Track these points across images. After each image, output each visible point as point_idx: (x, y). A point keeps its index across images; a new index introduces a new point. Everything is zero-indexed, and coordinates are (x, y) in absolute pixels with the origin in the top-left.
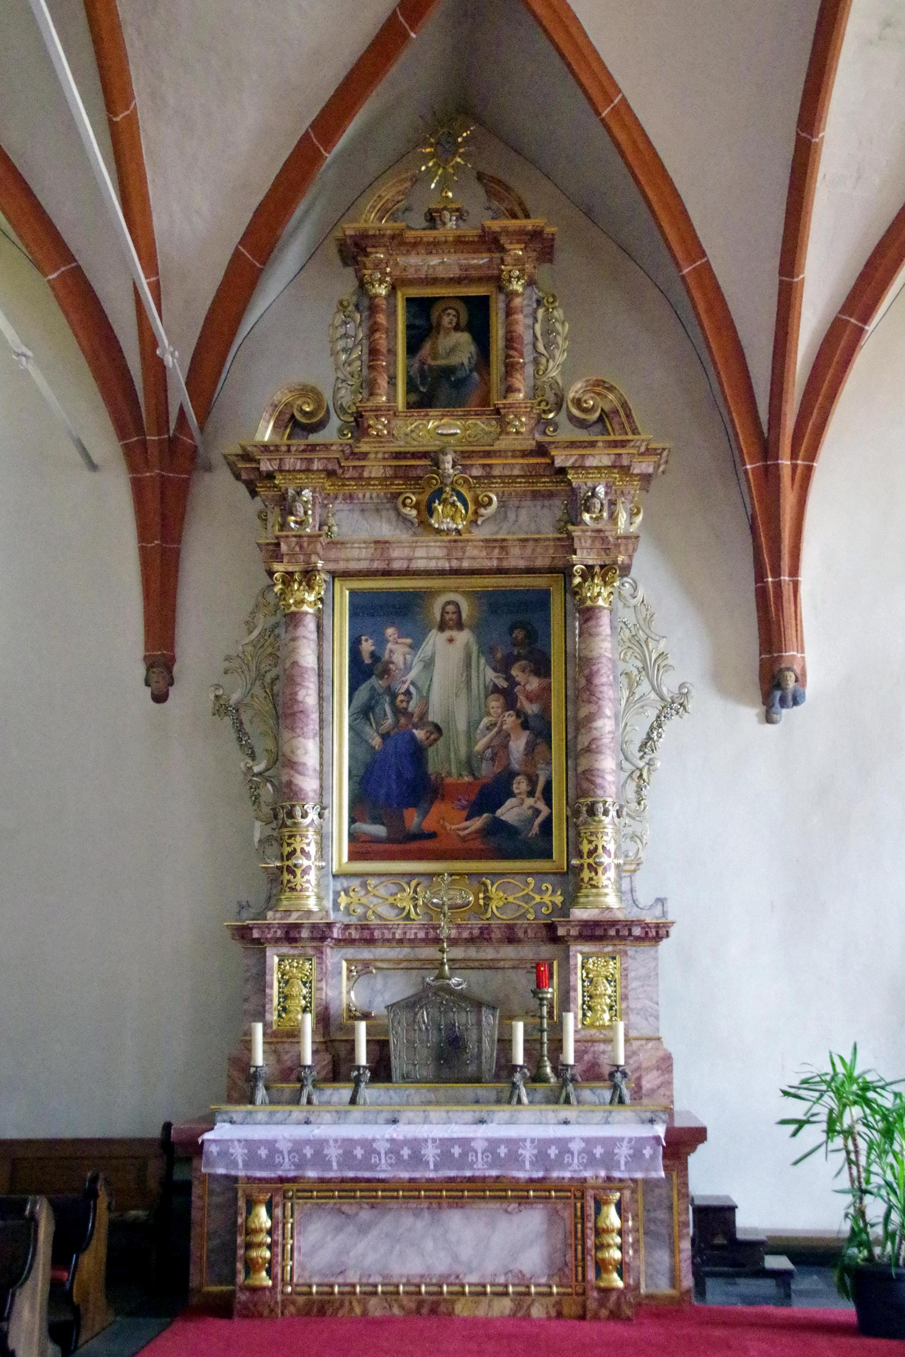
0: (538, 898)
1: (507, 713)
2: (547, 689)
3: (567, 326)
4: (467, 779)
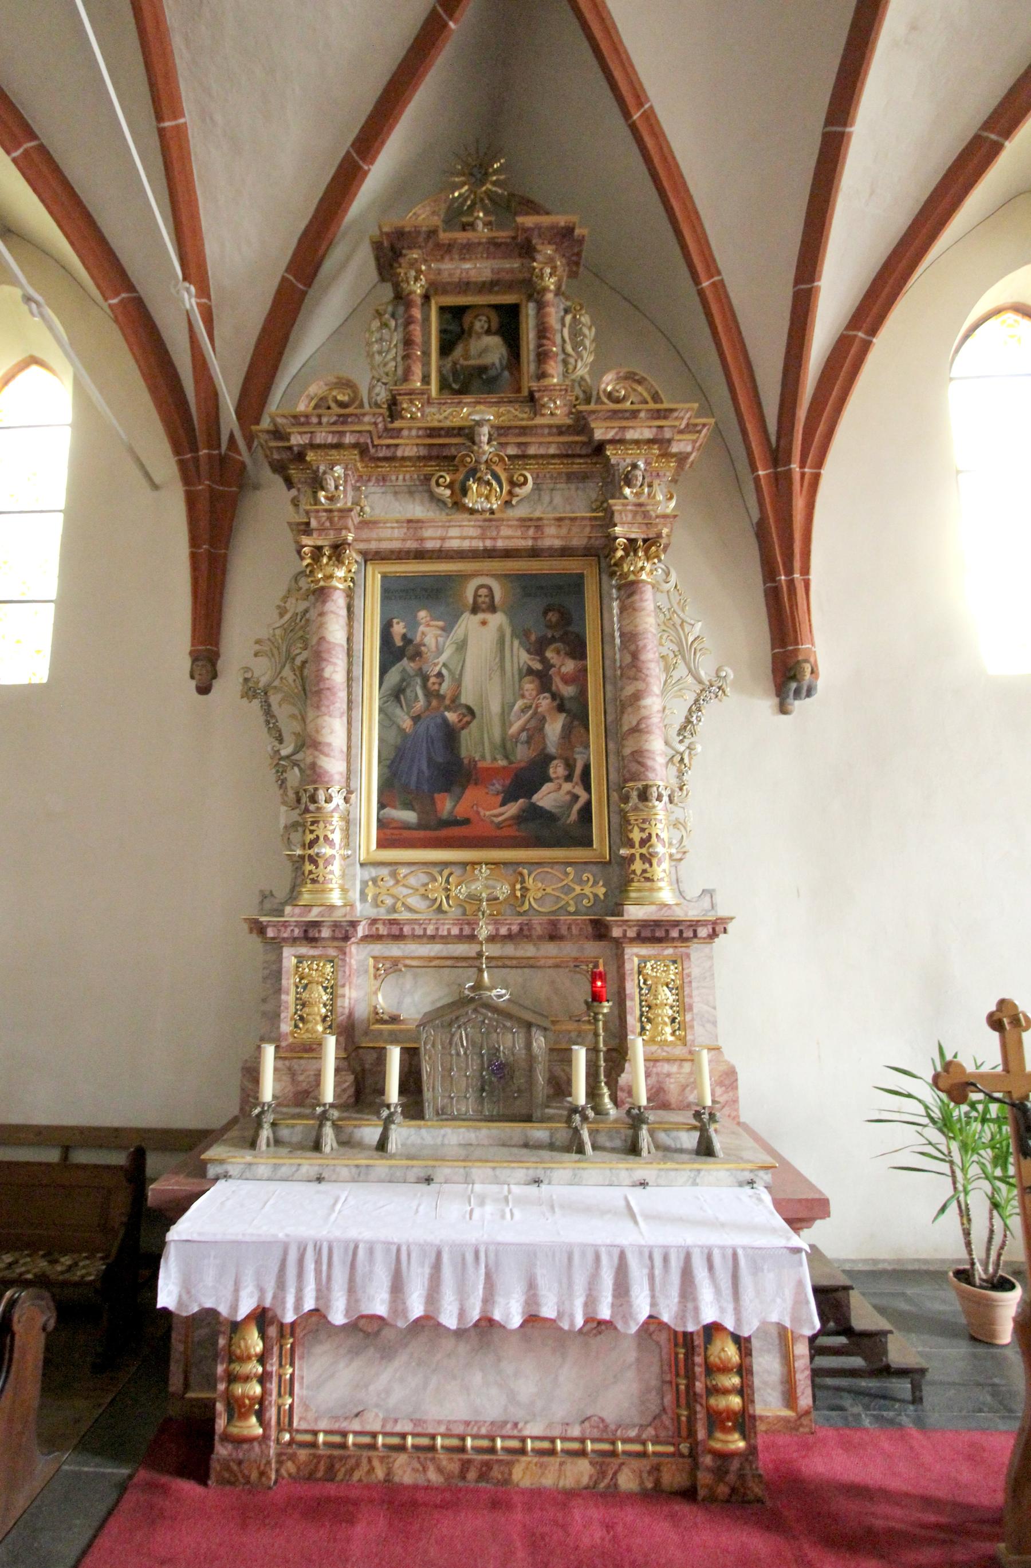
0: (578, 889)
1: (542, 696)
2: (584, 670)
3: (593, 330)
4: (502, 763)
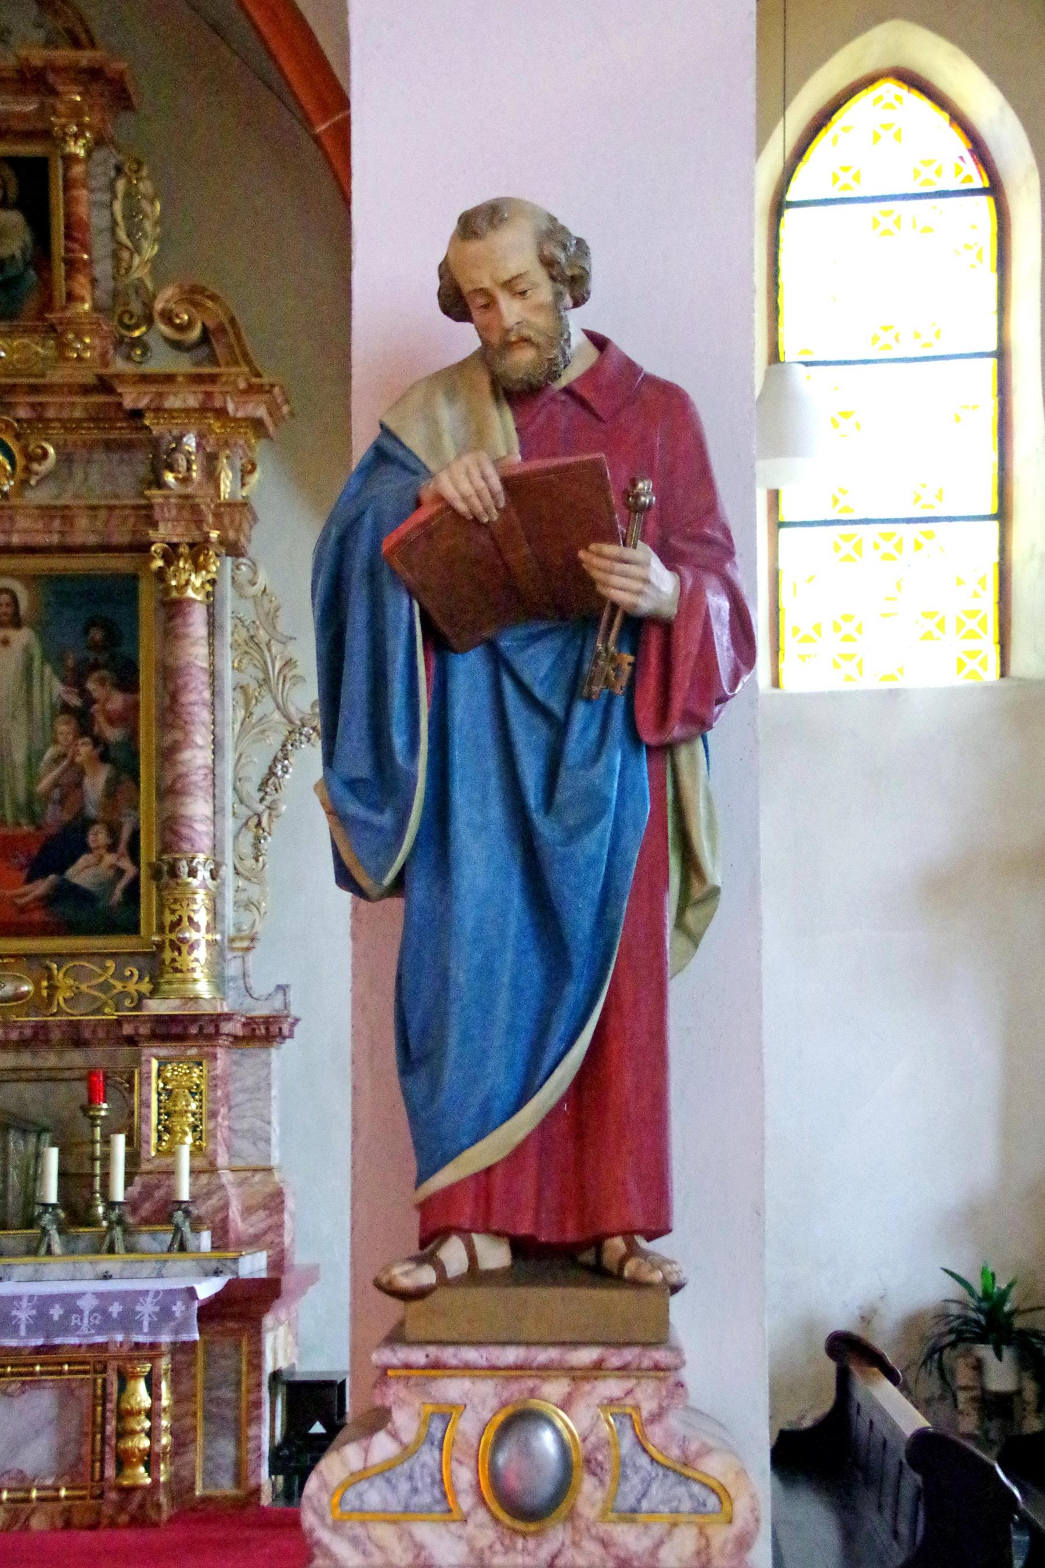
1: (80, 742)
2: (136, 706)
4: (26, 828)
